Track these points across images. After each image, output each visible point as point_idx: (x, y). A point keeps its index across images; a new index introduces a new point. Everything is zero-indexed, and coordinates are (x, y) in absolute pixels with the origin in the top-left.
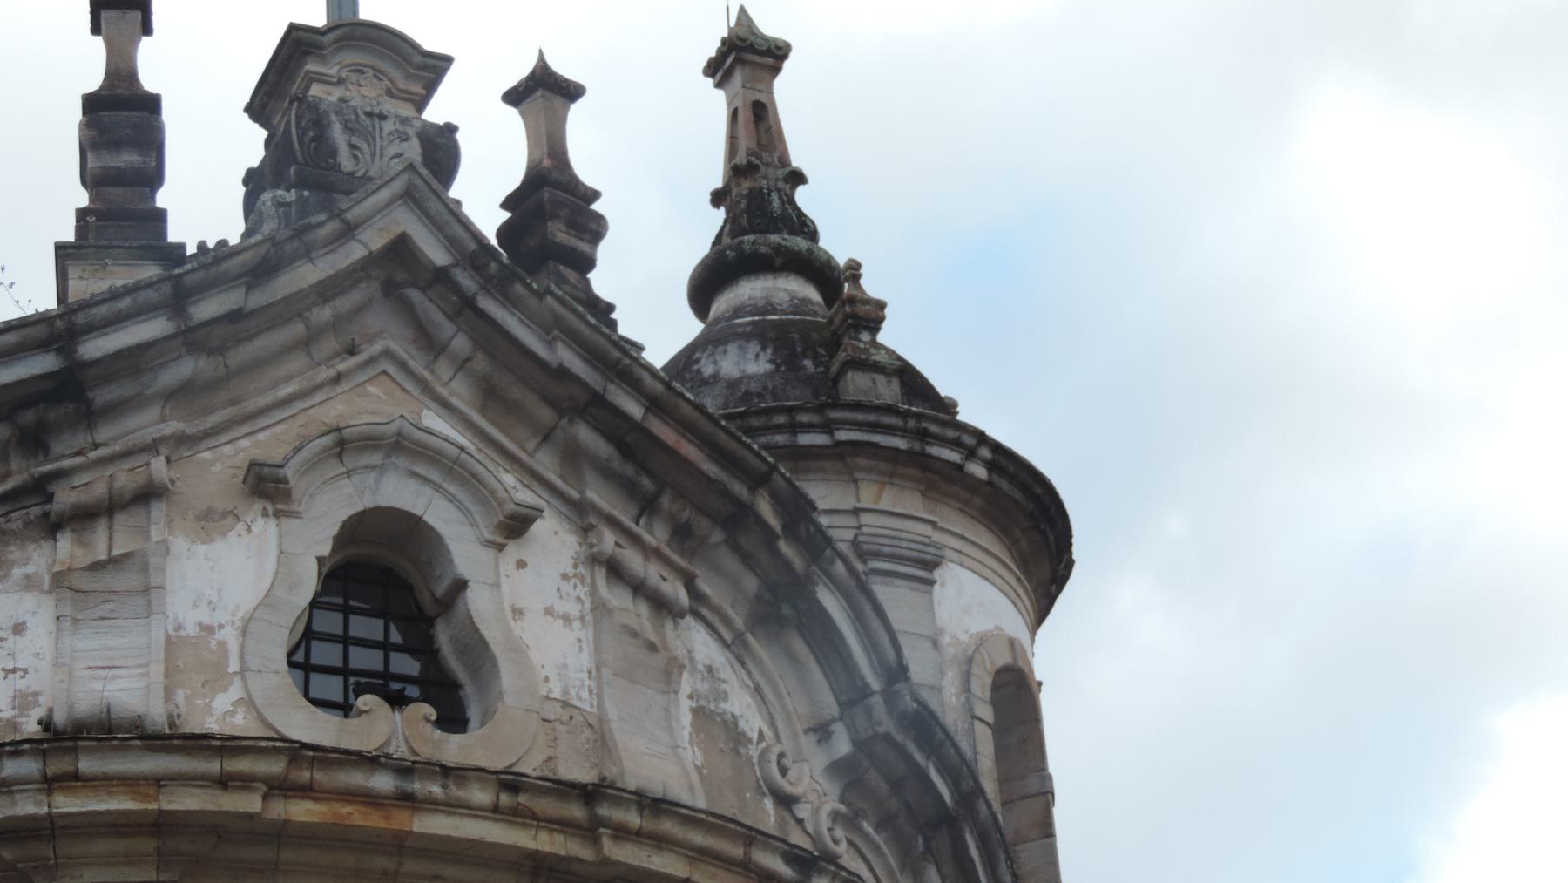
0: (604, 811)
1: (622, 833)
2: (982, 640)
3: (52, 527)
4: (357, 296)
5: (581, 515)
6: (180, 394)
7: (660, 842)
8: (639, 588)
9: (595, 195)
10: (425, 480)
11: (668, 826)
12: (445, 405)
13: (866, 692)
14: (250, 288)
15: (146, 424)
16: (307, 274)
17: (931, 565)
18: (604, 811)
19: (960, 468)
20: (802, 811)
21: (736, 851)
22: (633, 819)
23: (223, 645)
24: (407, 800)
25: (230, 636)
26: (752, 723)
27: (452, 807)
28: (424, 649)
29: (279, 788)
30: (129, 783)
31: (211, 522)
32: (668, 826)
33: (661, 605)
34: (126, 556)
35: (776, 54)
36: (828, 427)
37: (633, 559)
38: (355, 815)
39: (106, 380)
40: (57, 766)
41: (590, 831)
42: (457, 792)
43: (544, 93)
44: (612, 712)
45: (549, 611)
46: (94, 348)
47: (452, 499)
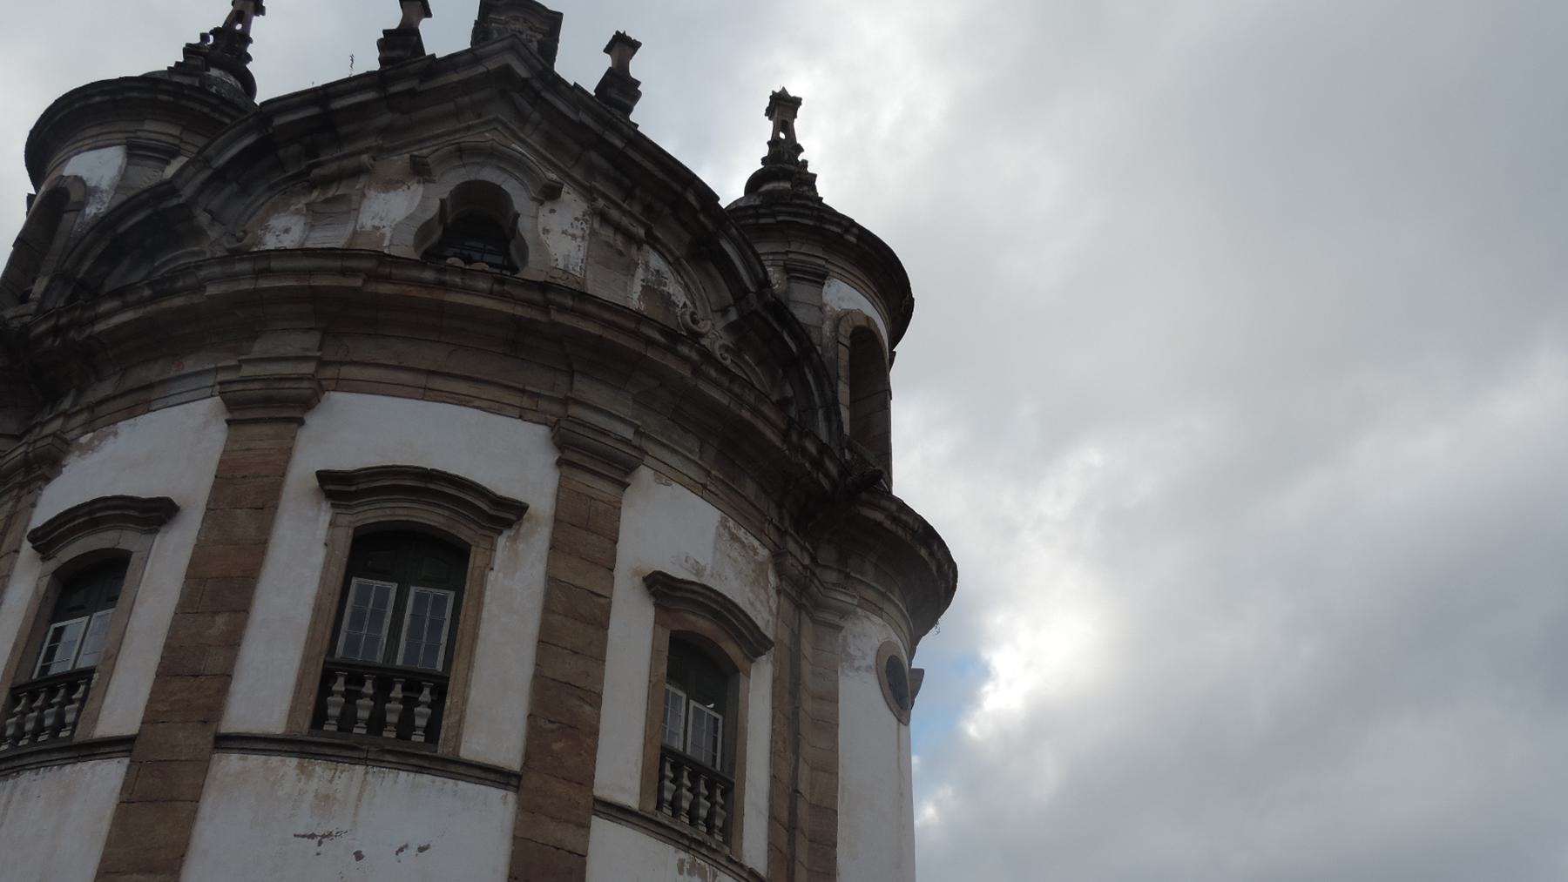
0: (552, 296)
1: (562, 309)
2: (848, 312)
3: (313, 185)
5: (589, 193)
6: (386, 131)
7: (585, 316)
8: (618, 228)
9: (638, 83)
10: (504, 170)
11: (589, 308)
12: (523, 142)
13: (747, 291)
14: (422, 82)
16: (454, 77)
18: (552, 296)
19: (841, 236)
21: (632, 325)
22: (569, 302)
23: (383, 235)
24: (441, 285)
25: (388, 232)
26: (680, 297)
27: (466, 290)
28: (507, 255)
29: (371, 276)
31: (390, 185)
32: (589, 308)
33: (630, 237)
34: (342, 196)
35: (797, 102)
36: (774, 215)
37: (614, 214)
38: (414, 291)
40: (261, 265)
41: (545, 307)
43: (622, 46)
44: (589, 276)
45: (564, 232)
46: (337, 104)
47: (517, 179)
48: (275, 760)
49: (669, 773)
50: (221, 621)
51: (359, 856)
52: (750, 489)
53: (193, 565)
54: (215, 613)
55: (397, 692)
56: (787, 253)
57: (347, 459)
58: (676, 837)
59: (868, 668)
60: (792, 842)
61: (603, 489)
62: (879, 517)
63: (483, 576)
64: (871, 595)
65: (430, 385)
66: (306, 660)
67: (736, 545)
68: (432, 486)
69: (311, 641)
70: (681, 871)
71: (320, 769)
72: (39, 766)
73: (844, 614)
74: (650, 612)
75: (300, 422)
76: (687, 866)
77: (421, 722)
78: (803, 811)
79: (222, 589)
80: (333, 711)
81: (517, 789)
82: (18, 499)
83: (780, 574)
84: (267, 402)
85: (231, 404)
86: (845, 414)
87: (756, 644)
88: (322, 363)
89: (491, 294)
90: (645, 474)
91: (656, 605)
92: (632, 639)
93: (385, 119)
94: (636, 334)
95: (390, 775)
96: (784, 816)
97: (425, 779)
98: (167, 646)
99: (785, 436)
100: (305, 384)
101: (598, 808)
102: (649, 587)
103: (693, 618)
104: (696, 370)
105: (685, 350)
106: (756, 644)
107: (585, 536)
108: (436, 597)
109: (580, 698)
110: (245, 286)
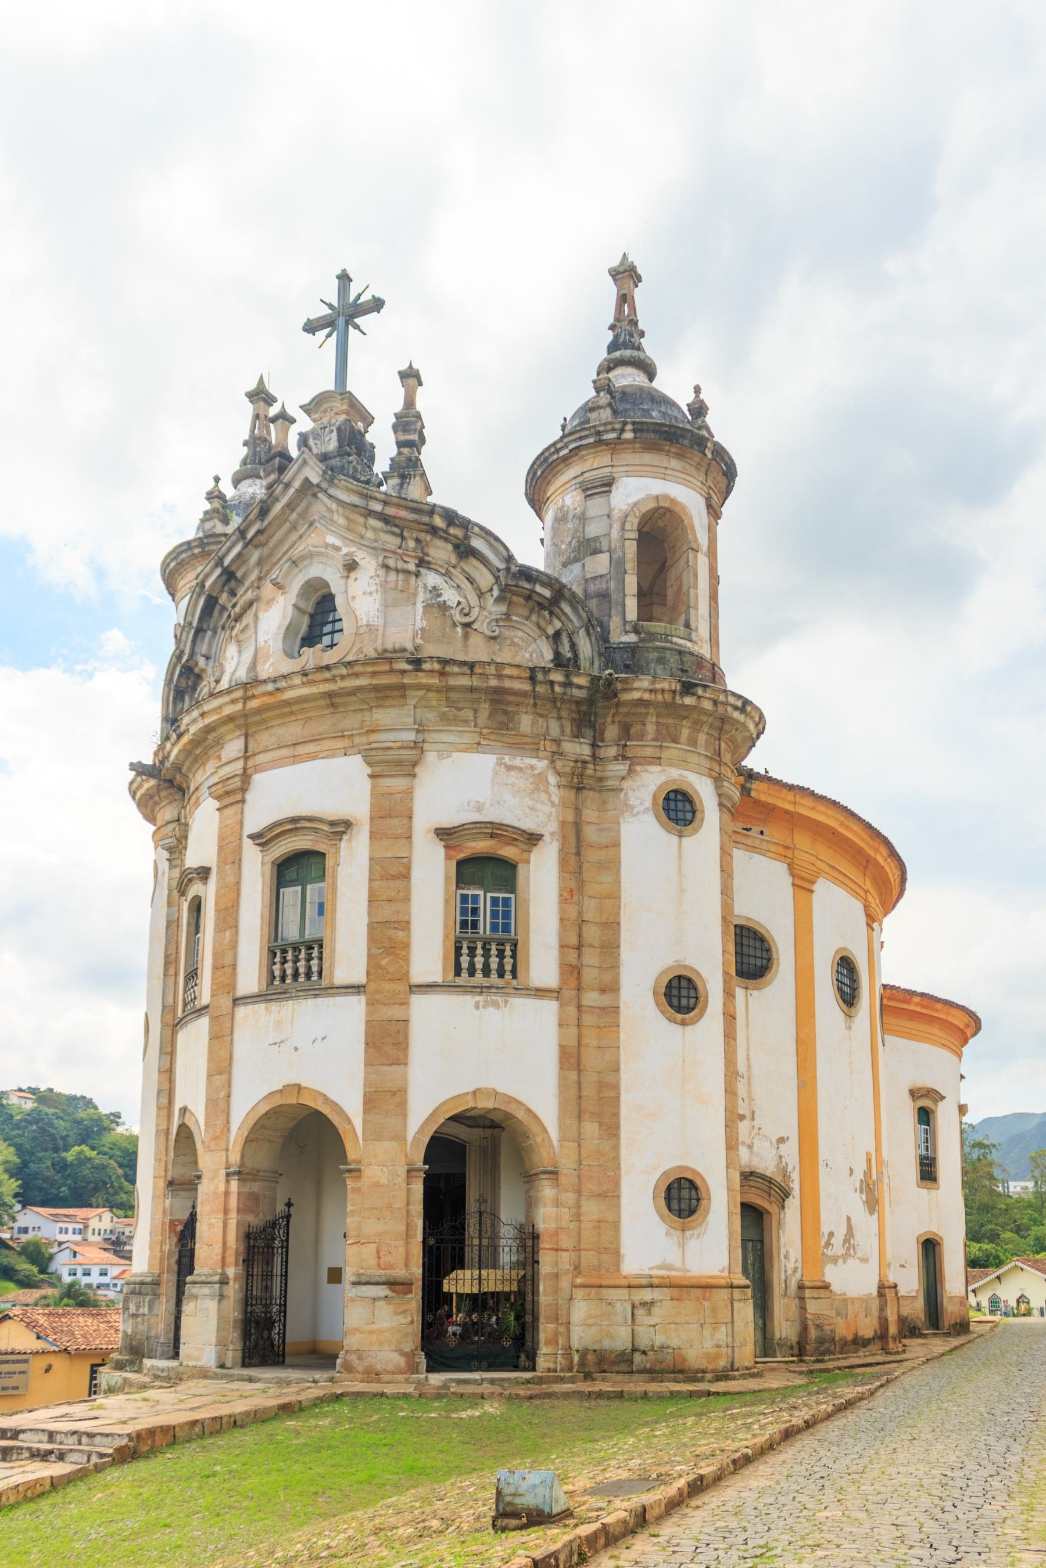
2: (635, 504)
4: (303, 505)
17: (609, 484)
27: (291, 687)
29: (246, 699)
31: (270, 602)
38: (267, 700)
42: (290, 683)
45: (364, 593)
48: (257, 1006)
49: (465, 951)
51: (296, 1049)
52: (526, 722)
55: (302, 955)
56: (582, 474)
58: (470, 989)
59: (647, 809)
61: (398, 783)
62: (636, 695)
63: (334, 871)
66: (261, 948)
67: (512, 773)
68: (298, 825)
70: (477, 1007)
71: (274, 1006)
74: (442, 852)
76: (482, 1004)
78: (592, 933)
80: (277, 973)
87: (533, 839)
90: (431, 757)
91: (445, 847)
92: (431, 875)
93: (255, 556)
95: (303, 1002)
96: (573, 940)
97: (319, 1000)
101: (414, 989)
103: (473, 844)
106: (533, 839)
107: (391, 817)
109: (396, 928)
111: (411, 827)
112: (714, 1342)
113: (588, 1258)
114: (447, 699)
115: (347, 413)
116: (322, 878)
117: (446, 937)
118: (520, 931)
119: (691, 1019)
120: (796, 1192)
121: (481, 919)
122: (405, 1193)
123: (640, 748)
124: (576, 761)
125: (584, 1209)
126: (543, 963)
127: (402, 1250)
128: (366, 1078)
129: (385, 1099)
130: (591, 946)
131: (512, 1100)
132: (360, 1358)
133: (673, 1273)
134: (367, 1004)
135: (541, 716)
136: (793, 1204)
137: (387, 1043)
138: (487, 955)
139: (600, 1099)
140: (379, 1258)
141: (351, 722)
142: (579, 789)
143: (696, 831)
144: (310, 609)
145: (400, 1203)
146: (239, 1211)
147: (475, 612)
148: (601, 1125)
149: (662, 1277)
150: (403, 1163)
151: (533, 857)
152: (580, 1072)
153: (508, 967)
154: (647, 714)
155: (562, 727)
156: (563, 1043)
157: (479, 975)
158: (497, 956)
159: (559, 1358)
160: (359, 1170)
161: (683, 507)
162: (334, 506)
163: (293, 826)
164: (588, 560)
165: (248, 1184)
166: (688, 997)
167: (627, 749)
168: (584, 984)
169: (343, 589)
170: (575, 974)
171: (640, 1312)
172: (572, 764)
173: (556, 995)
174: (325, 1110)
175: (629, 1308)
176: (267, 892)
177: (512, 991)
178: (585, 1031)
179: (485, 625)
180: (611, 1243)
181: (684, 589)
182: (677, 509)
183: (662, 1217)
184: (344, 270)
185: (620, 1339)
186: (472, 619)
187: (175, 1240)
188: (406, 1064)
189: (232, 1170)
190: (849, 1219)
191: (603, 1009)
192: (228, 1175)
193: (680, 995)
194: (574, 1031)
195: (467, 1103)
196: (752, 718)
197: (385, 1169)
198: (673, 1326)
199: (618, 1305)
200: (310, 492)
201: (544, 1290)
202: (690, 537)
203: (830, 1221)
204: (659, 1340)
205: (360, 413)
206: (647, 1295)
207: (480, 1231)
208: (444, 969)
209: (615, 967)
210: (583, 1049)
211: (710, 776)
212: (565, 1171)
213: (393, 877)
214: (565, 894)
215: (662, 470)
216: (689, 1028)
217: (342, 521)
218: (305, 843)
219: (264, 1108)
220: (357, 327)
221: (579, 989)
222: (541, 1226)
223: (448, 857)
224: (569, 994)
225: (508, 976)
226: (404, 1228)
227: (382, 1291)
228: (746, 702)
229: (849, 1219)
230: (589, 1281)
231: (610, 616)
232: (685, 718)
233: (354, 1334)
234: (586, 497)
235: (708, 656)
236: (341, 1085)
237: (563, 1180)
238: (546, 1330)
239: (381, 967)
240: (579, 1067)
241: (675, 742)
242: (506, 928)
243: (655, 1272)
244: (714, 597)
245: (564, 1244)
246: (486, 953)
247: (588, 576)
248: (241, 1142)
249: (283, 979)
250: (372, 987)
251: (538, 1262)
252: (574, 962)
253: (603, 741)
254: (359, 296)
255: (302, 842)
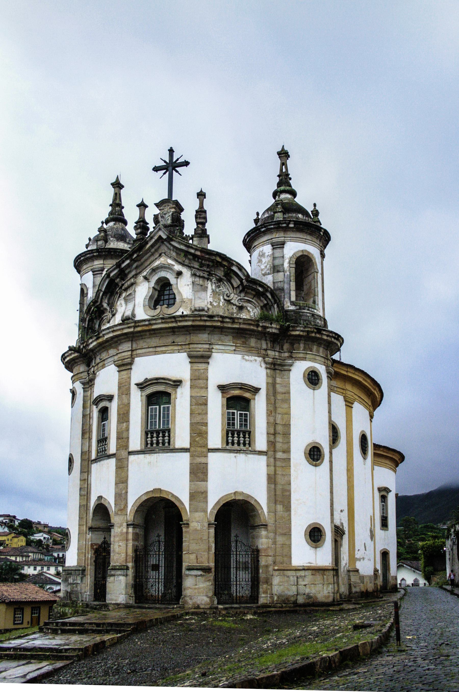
1: (180, 321)
6: (137, 268)
8: (200, 277)
13: (243, 279)
15: (133, 273)
17: (284, 244)
20: (232, 301)
21: (199, 319)
22: (181, 319)
29: (135, 327)
30: (120, 330)
36: (265, 227)
39: (126, 269)
41: (176, 322)
49: (230, 435)
50: (125, 424)
53: (118, 411)
54: (123, 423)
55: (161, 435)
57: (141, 380)
60: (275, 438)
61: (202, 366)
62: (297, 333)
63: (175, 401)
64: (301, 355)
65: (156, 350)
66: (141, 431)
68: (159, 381)
69: (142, 426)
72: (104, 460)
73: (291, 365)
74: (219, 394)
75: (131, 369)
77: (167, 441)
78: (280, 429)
79: (124, 417)
80: (149, 442)
81: (189, 452)
82: (91, 389)
83: (266, 363)
84: (123, 365)
85: (118, 366)
86: (293, 294)
87: (256, 390)
88: (132, 351)
89: (162, 323)
90: (214, 354)
91: (222, 392)
94: (201, 320)
96: (272, 431)
98: (117, 432)
99: (258, 326)
100: (129, 359)
102: (219, 388)
103: (233, 392)
104: (222, 322)
105: (216, 319)
108: (167, 407)
110: (111, 335)
111: (207, 384)
112: (328, 591)
113: (279, 559)
114: (222, 331)
115: (175, 208)
116: (169, 403)
117: (223, 430)
118: (252, 428)
119: (318, 464)
120: (347, 532)
121: (236, 422)
122: (207, 533)
123: (298, 354)
124: (274, 358)
125: (277, 540)
126: (261, 441)
127: (206, 556)
128: (190, 487)
129: (198, 496)
130: (279, 433)
131: (249, 496)
132: (191, 599)
133: (312, 565)
134: (191, 456)
135: (258, 339)
136: (346, 538)
137: (199, 472)
138: (239, 437)
139: (283, 495)
140: (197, 559)
141: (180, 339)
142: (275, 369)
143: (319, 388)
144: (159, 289)
145: (205, 537)
146: (133, 540)
147: (232, 295)
148: (283, 506)
149: (308, 566)
150: (207, 521)
151: (257, 397)
152: (275, 484)
153: (247, 442)
154: (301, 340)
155: (267, 344)
156: (269, 473)
157: (236, 445)
158: (243, 438)
159: (268, 598)
160: (188, 524)
161: (312, 255)
162: (172, 248)
163: (156, 381)
164: (276, 274)
165: (135, 529)
166: (317, 455)
167: (293, 354)
168: (277, 449)
169: (176, 282)
170: (273, 445)
171: (300, 580)
172: (271, 360)
173: (265, 454)
174: (173, 500)
175: (296, 579)
176: (144, 408)
177: (249, 452)
178: (277, 469)
179: (236, 301)
180: (288, 553)
181: (313, 288)
182: (310, 256)
183: (308, 543)
184: (171, 148)
185: (292, 591)
186: (231, 298)
187: (93, 552)
188: (207, 481)
189: (129, 523)
190: (365, 544)
191: (284, 459)
192: (128, 525)
193: (314, 454)
194: (273, 468)
195: (232, 497)
196: (340, 342)
197: (199, 524)
198: (313, 585)
199: (291, 578)
200: (161, 241)
201: (262, 572)
202: (315, 267)
203: (358, 545)
204: (307, 591)
205: (179, 208)
206: (302, 573)
207: (236, 549)
208: (222, 442)
209: (289, 442)
210: (277, 476)
211: (324, 365)
212: (270, 525)
213: (201, 405)
214: (269, 412)
215: (304, 240)
216: (317, 468)
217: (174, 254)
218: (161, 388)
219: (145, 498)
220: (177, 171)
221: (275, 451)
222: (260, 547)
223: (223, 397)
224: (271, 453)
225: (247, 446)
226: (207, 547)
227: (199, 573)
228: (339, 336)
229: (365, 544)
230: (280, 568)
231: (284, 298)
232: (316, 342)
233: (188, 590)
234: (273, 248)
235: (322, 316)
236: (179, 488)
237: (269, 528)
238: (263, 587)
239: (195, 441)
240: (275, 484)
241: (311, 351)
242: (246, 425)
243: (305, 565)
244: (323, 291)
245: (270, 554)
246: (238, 437)
247: (275, 281)
248: (134, 512)
249: (152, 444)
250: (192, 449)
251: (259, 561)
252: (273, 440)
253: (283, 350)
254: (178, 160)
255: (161, 388)
